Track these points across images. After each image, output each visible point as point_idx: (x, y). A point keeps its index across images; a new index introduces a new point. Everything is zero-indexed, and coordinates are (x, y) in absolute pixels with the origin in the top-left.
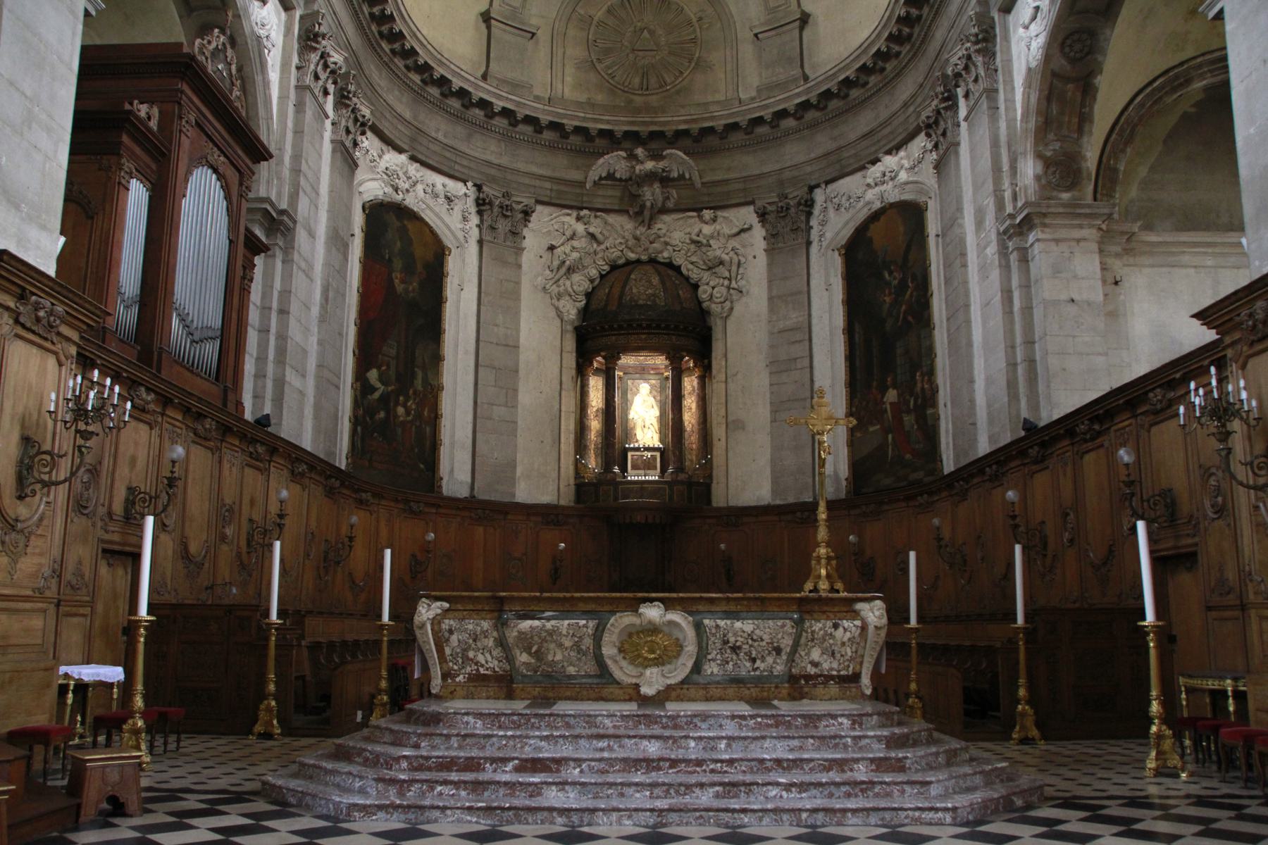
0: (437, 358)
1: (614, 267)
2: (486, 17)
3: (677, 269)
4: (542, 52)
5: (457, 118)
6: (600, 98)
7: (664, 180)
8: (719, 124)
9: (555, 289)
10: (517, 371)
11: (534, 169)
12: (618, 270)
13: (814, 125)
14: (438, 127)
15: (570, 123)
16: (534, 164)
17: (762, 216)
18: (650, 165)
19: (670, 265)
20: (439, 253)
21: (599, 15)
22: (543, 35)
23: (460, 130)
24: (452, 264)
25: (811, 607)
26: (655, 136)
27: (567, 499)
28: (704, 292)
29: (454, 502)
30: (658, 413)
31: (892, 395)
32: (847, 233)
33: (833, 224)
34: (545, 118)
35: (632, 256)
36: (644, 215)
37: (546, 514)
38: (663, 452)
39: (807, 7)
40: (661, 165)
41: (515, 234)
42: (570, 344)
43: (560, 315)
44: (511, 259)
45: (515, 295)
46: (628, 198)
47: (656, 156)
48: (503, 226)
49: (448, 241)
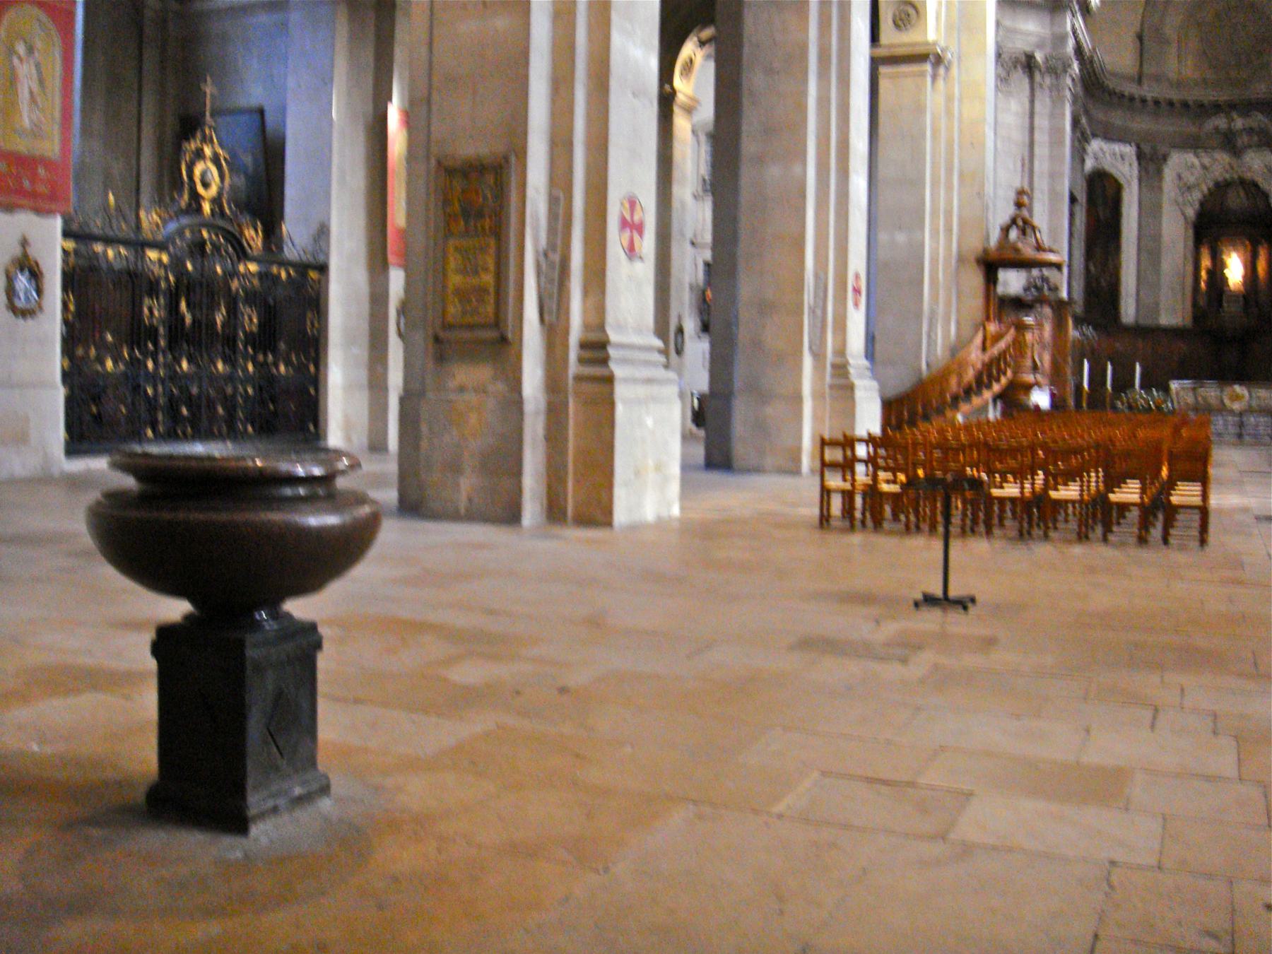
1: (1217, 185)
2: (1140, 37)
3: (1255, 185)
4: (1173, 50)
6: (1210, 75)
7: (1250, 131)
12: (1221, 188)
14: (1118, 118)
16: (1168, 126)
20: (1118, 188)
29: (1127, 329)
35: (1228, 176)
36: (1236, 152)
37: (1175, 333)
38: (1244, 297)
41: (1159, 172)
42: (1191, 232)
43: (1185, 218)
44: (1156, 184)
46: (1229, 143)
48: (1151, 167)
49: (1122, 181)
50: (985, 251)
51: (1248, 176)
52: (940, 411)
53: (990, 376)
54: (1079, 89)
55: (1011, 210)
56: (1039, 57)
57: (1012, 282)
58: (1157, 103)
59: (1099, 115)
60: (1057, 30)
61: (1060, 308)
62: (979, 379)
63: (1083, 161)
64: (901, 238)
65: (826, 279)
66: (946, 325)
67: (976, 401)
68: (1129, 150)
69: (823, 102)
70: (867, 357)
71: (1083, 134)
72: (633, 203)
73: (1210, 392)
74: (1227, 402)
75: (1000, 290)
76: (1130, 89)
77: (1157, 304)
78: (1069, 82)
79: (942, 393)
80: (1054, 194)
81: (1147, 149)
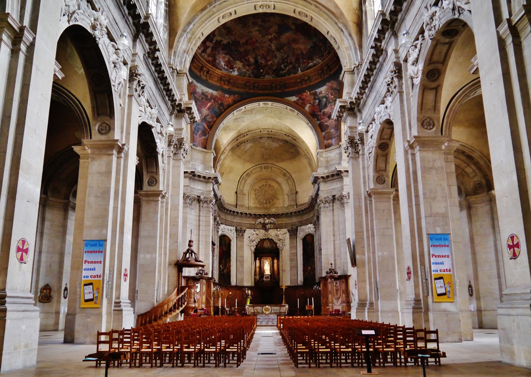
0: (230, 261)
1: (261, 240)
2: (236, 193)
5: (232, 215)
6: (258, 206)
7: (271, 223)
8: (281, 213)
9: (250, 245)
10: (243, 261)
11: (246, 222)
12: (262, 241)
13: (298, 215)
14: (229, 218)
15: (252, 213)
17: (289, 231)
18: (267, 221)
19: (272, 239)
20: (230, 240)
21: (258, 188)
22: (247, 194)
23: (233, 217)
24: (232, 243)
25: (281, 306)
26: (268, 215)
27: (253, 285)
28: (278, 245)
29: (233, 286)
30: (269, 267)
31: (309, 268)
32: (303, 236)
33: (301, 235)
34: (248, 213)
36: (266, 230)
39: (297, 190)
40: (270, 221)
41: (243, 235)
42: (253, 255)
45: (242, 247)
46: (264, 226)
47: (269, 218)
48: (240, 234)
49: (231, 239)
50: (178, 261)
51: (270, 238)
52: (160, 318)
53: (178, 306)
54: (216, 208)
55: (187, 247)
56: (202, 197)
57: (189, 272)
58: (241, 213)
59: (223, 216)
60: (208, 189)
61: (209, 280)
62: (174, 306)
63: (218, 232)
64: (148, 256)
65: (114, 270)
66: (160, 287)
67: (174, 314)
68: (233, 228)
69: (115, 208)
70: (129, 299)
71: (218, 223)
72: (24, 242)
73: (259, 308)
74: (265, 312)
75: (183, 274)
76: (233, 209)
77: (243, 279)
78: (212, 206)
79: (161, 312)
80: (207, 242)
81: (238, 228)
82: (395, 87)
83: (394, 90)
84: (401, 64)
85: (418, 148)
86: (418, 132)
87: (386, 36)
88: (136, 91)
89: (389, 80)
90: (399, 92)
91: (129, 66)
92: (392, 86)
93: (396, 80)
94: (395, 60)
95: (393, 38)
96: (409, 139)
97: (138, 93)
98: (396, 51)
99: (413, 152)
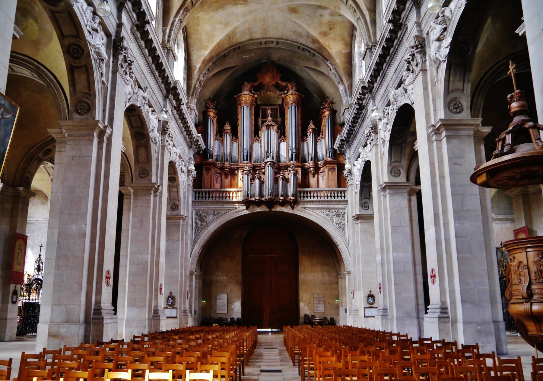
82: (417, 65)
83: (415, 68)
84: (424, 38)
85: (444, 134)
86: (445, 114)
87: (407, 6)
88: (122, 67)
89: (410, 57)
90: (421, 70)
91: (113, 38)
92: (414, 64)
93: (418, 56)
94: (417, 34)
95: (414, 8)
96: (433, 123)
97: (124, 69)
98: (419, 24)
99: (439, 139)
